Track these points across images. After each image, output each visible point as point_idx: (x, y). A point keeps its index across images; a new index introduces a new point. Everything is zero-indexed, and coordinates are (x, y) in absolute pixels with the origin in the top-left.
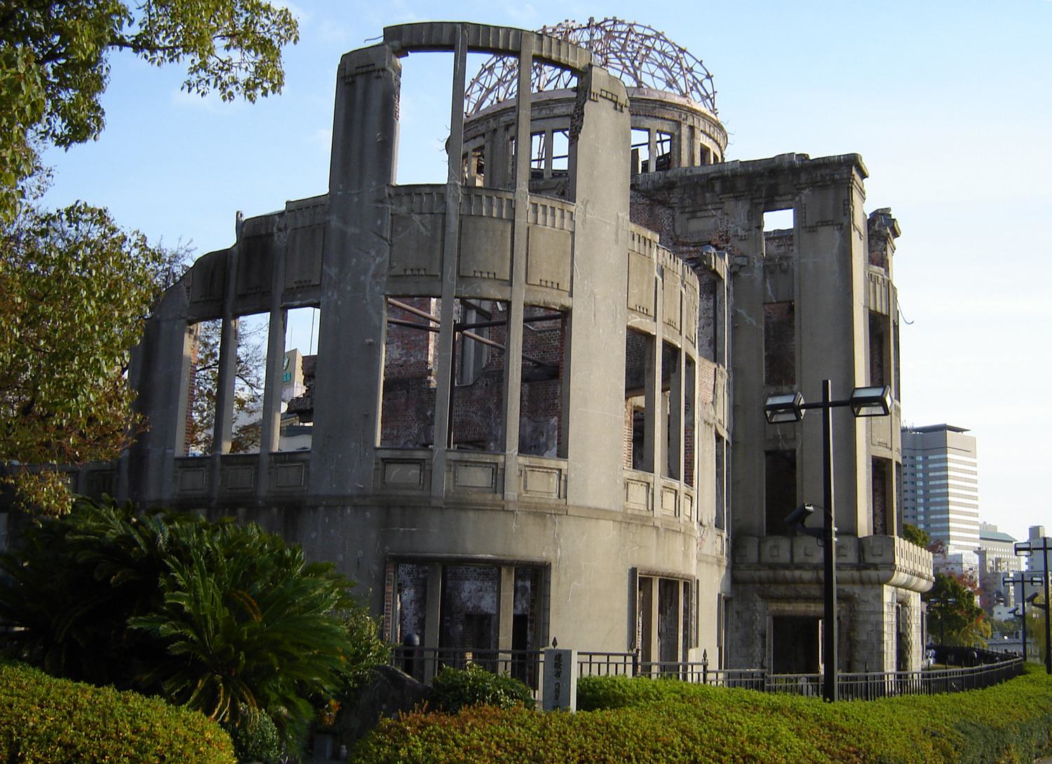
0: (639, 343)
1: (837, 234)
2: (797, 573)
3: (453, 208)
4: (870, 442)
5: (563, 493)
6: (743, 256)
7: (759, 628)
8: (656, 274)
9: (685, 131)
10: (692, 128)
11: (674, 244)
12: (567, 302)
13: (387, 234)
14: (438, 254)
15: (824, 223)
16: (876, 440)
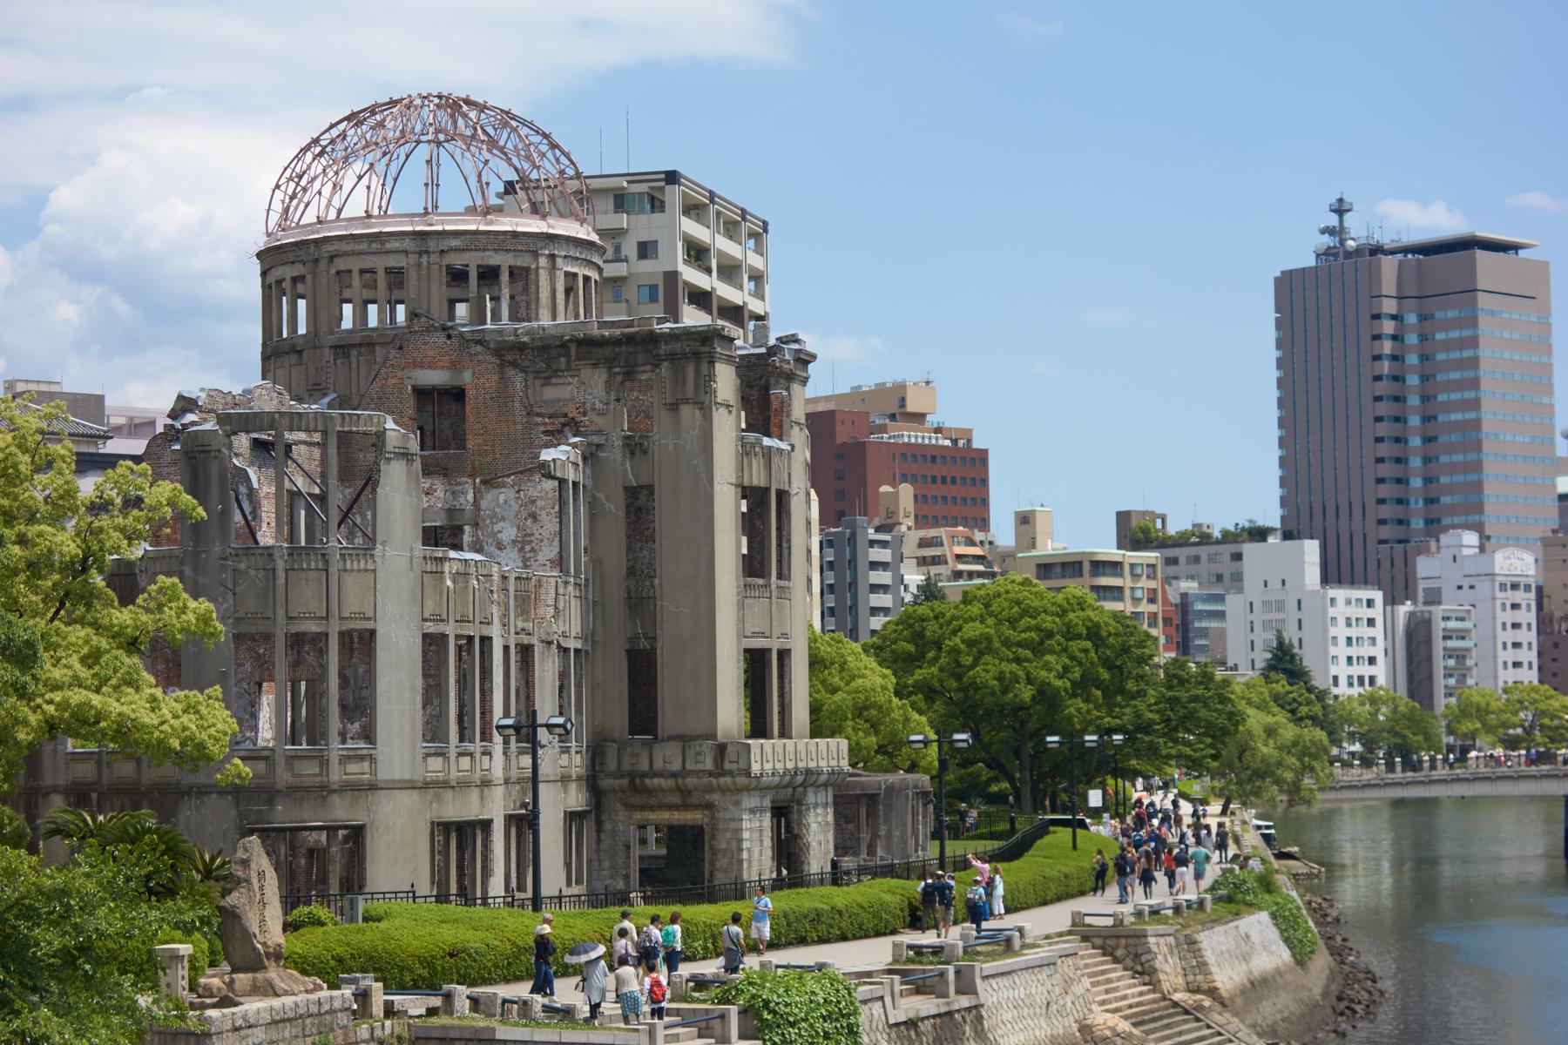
0: (433, 644)
1: (697, 412)
2: (656, 781)
3: (280, 565)
4: (742, 634)
5: (374, 772)
6: (600, 432)
7: (623, 839)
8: (449, 583)
9: (543, 261)
10: (552, 257)
11: (528, 414)
12: (369, 625)
13: (230, 585)
14: (271, 602)
15: (686, 401)
16: (749, 630)
